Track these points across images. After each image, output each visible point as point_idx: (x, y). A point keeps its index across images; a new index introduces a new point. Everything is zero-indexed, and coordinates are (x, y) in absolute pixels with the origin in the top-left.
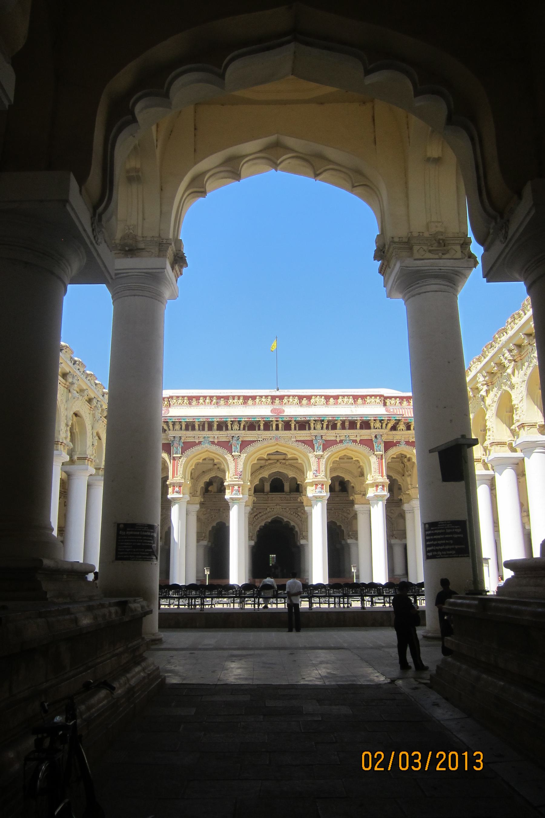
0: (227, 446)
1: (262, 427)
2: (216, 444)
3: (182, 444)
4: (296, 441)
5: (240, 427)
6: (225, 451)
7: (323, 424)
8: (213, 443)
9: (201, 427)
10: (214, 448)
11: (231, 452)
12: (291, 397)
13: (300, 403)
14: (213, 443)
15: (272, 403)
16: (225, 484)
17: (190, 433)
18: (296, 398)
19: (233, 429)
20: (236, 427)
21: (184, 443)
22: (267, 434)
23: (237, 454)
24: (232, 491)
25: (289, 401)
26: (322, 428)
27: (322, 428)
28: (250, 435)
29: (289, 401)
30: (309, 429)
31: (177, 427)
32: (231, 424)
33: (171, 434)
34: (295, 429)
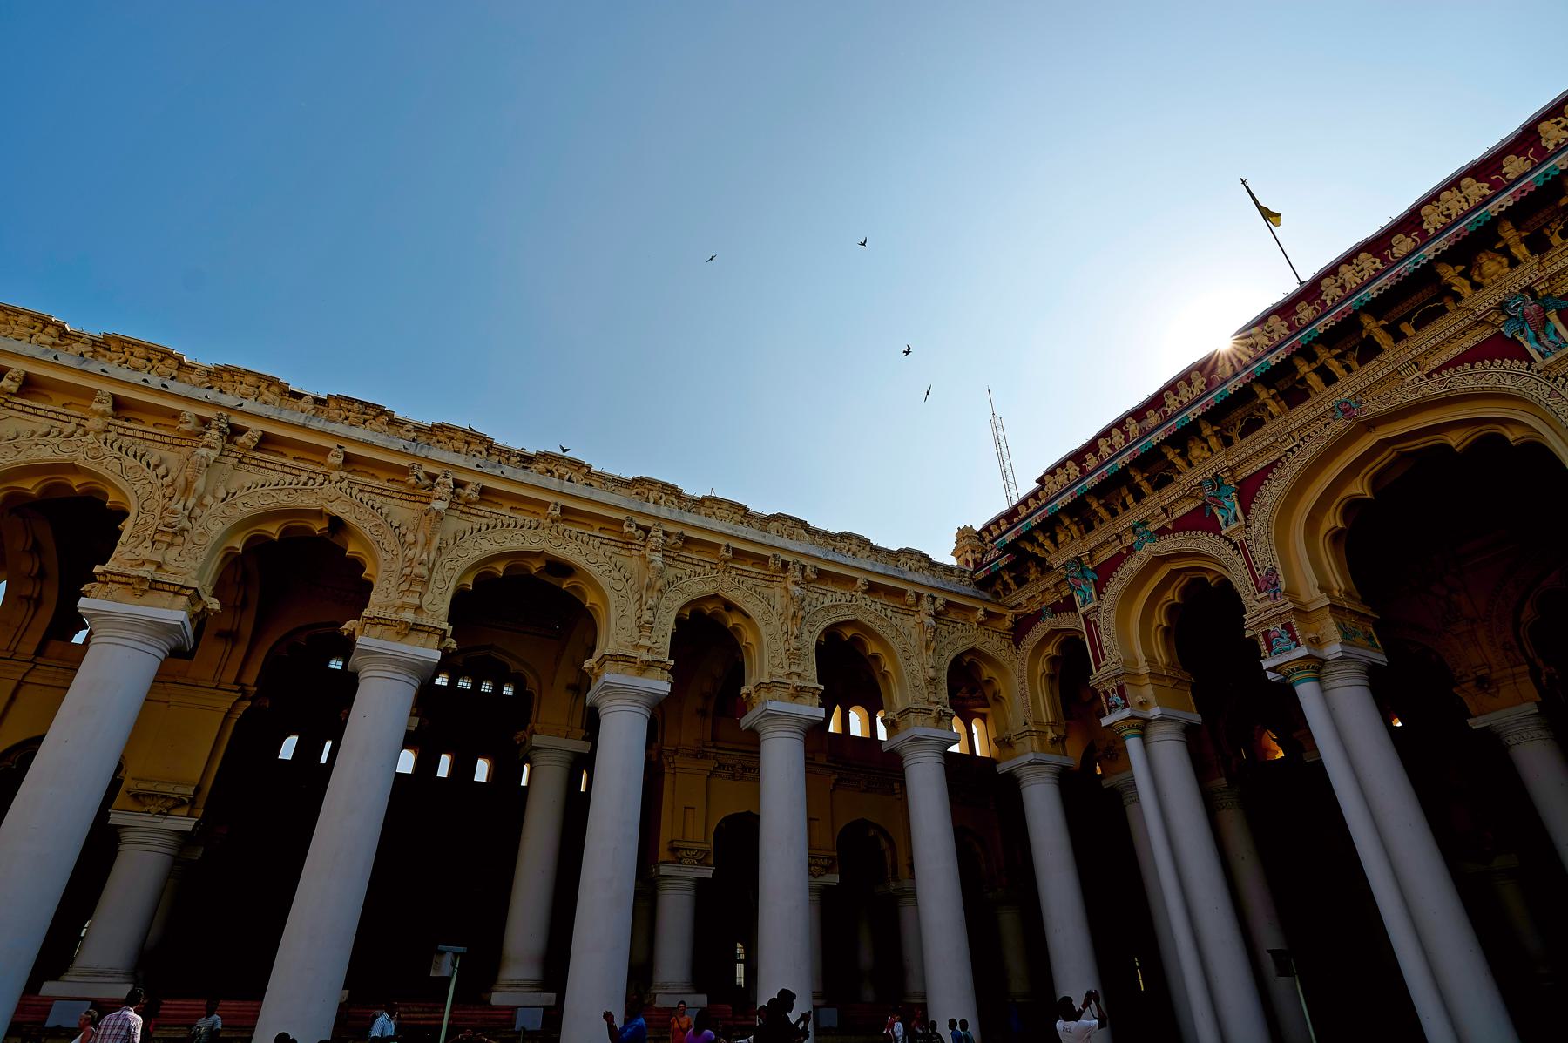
0: (1201, 520)
1: (1273, 407)
2: (1169, 532)
3: (1090, 575)
4: (1429, 376)
5: (1210, 449)
6: (1202, 536)
7: (1506, 251)
8: (1162, 532)
9: (1119, 509)
10: (1169, 544)
11: (1214, 528)
12: (1343, 268)
13: (1384, 260)
14: (1162, 532)
15: (1289, 328)
16: (1248, 634)
17: (1094, 539)
18: (1363, 256)
19: (1195, 463)
20: (1196, 451)
21: (1095, 570)
22: (1303, 413)
23: (1234, 525)
24: (1270, 648)
25: (1343, 287)
26: (1514, 262)
27: (1514, 262)
28: (1248, 454)
29: (1343, 287)
30: (1457, 297)
31: (1061, 538)
32: (1184, 455)
33: (1056, 560)
34: (1398, 337)
